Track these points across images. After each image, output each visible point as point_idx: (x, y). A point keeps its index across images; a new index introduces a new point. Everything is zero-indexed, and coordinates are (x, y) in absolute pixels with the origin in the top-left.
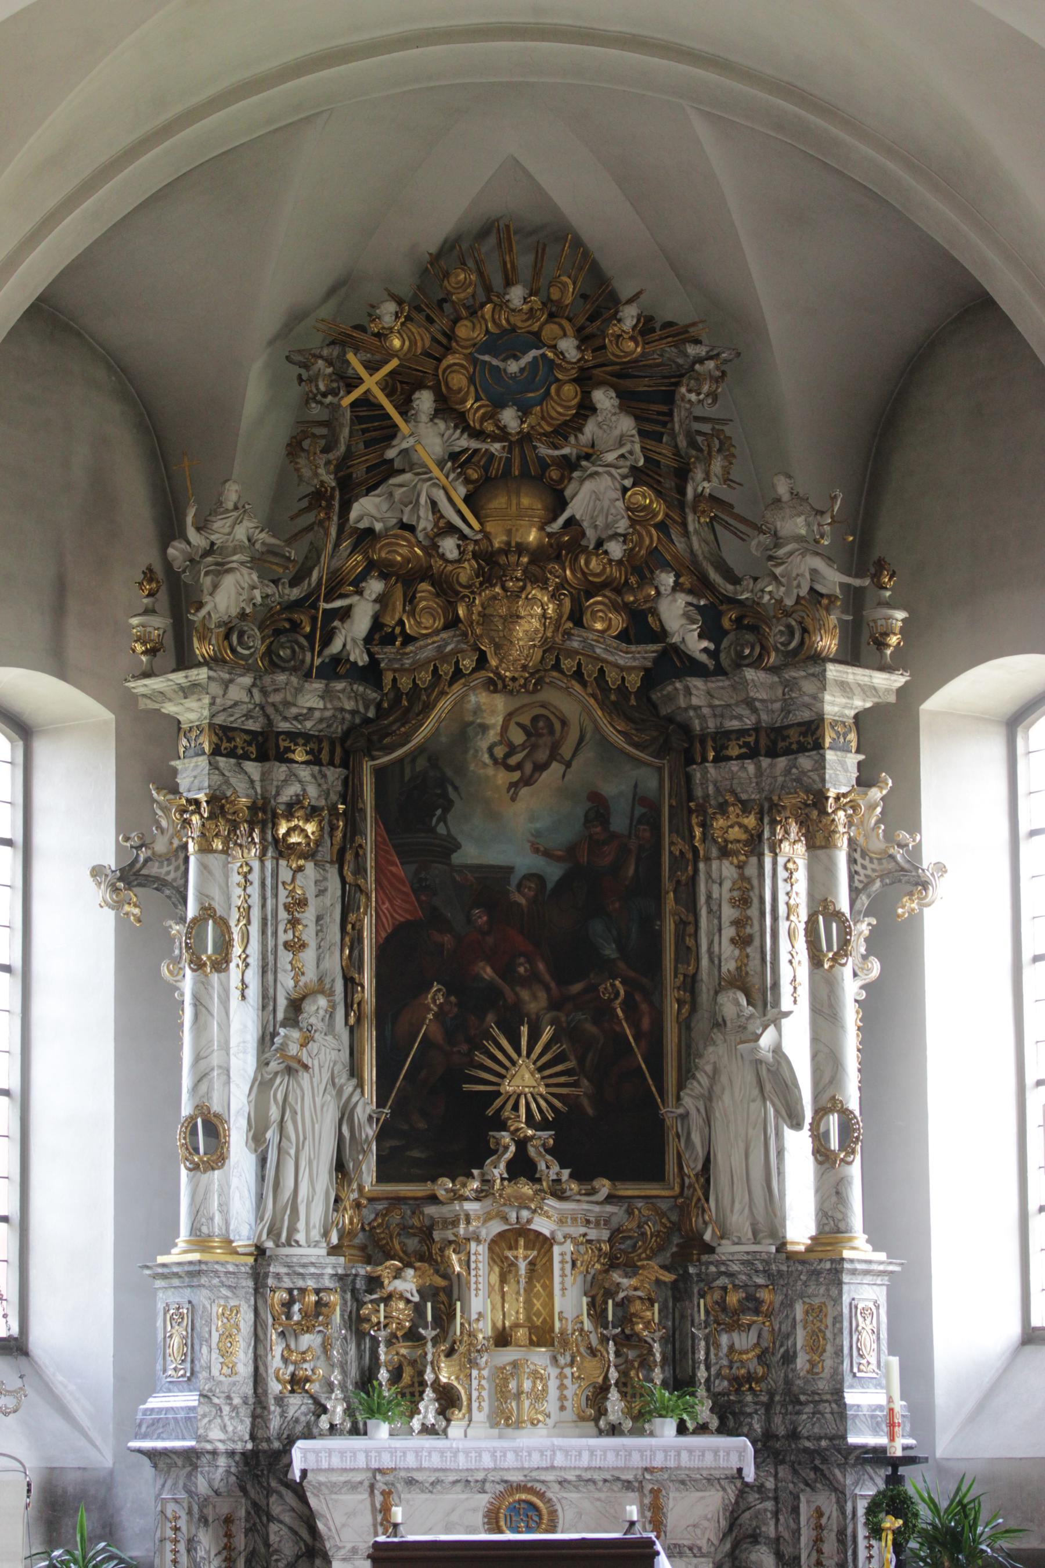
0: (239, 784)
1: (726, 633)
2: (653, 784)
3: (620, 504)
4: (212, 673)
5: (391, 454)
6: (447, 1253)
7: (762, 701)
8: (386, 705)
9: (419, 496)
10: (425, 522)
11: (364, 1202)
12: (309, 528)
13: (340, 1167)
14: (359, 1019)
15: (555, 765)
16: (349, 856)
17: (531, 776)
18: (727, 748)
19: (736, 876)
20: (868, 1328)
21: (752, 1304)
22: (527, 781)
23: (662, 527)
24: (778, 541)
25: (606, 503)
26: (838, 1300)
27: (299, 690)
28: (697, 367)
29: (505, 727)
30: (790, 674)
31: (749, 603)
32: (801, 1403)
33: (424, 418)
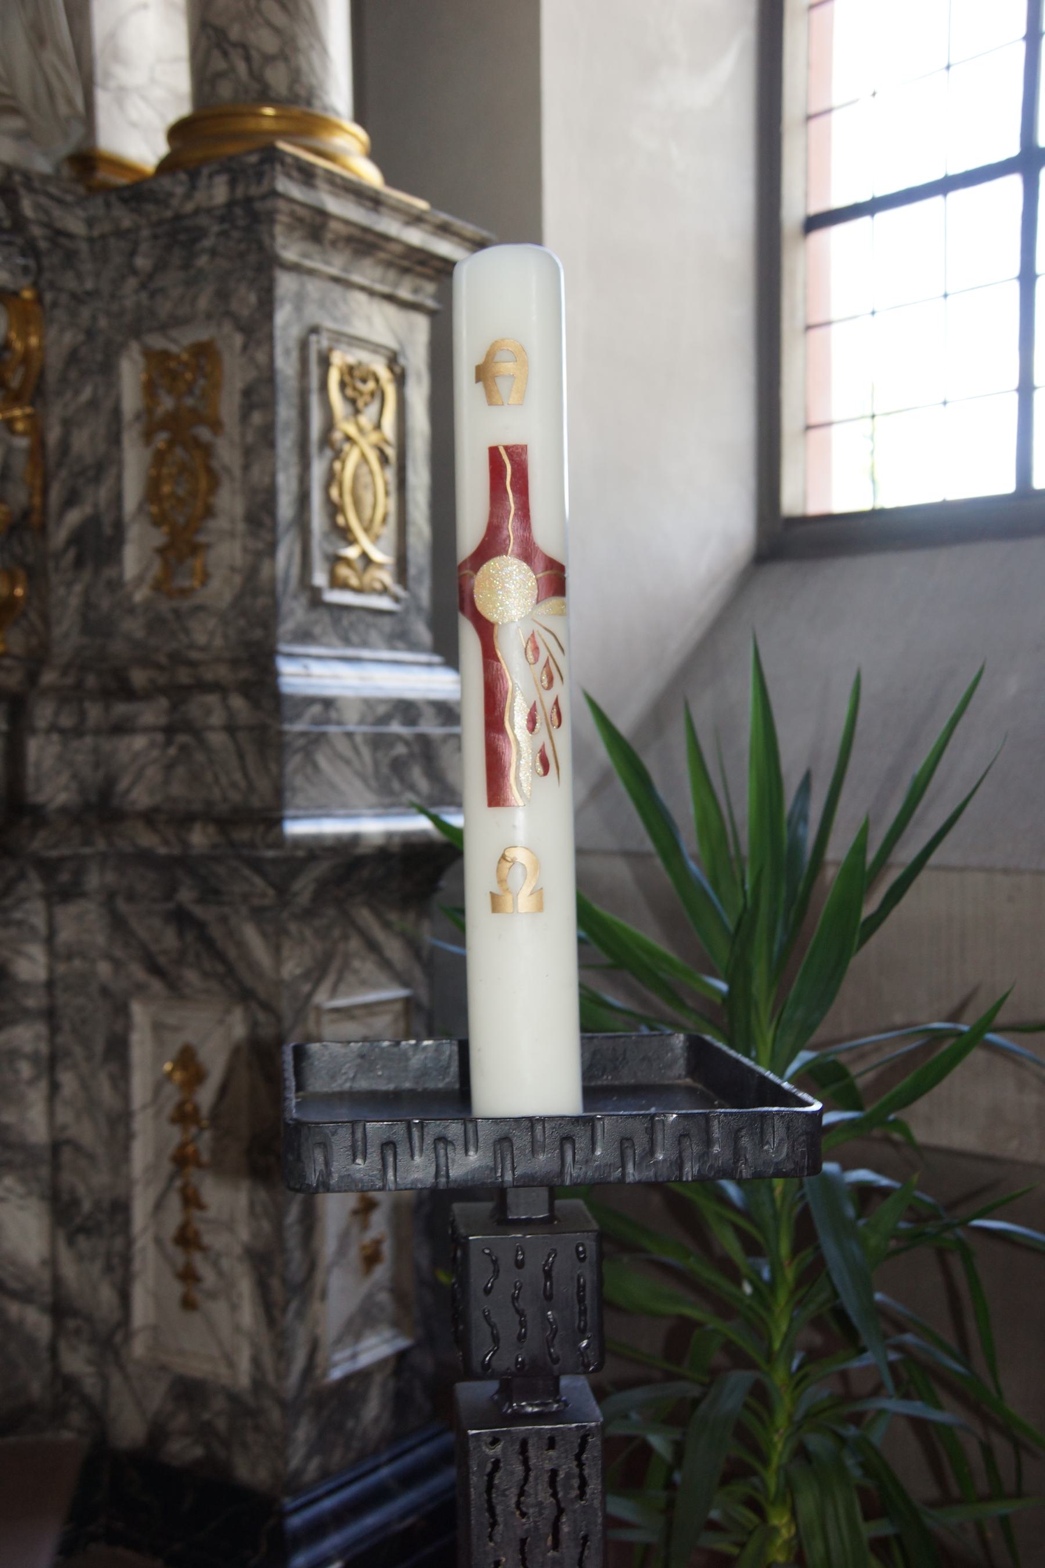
20: (366, 444)
26: (258, 329)
32: (129, 694)
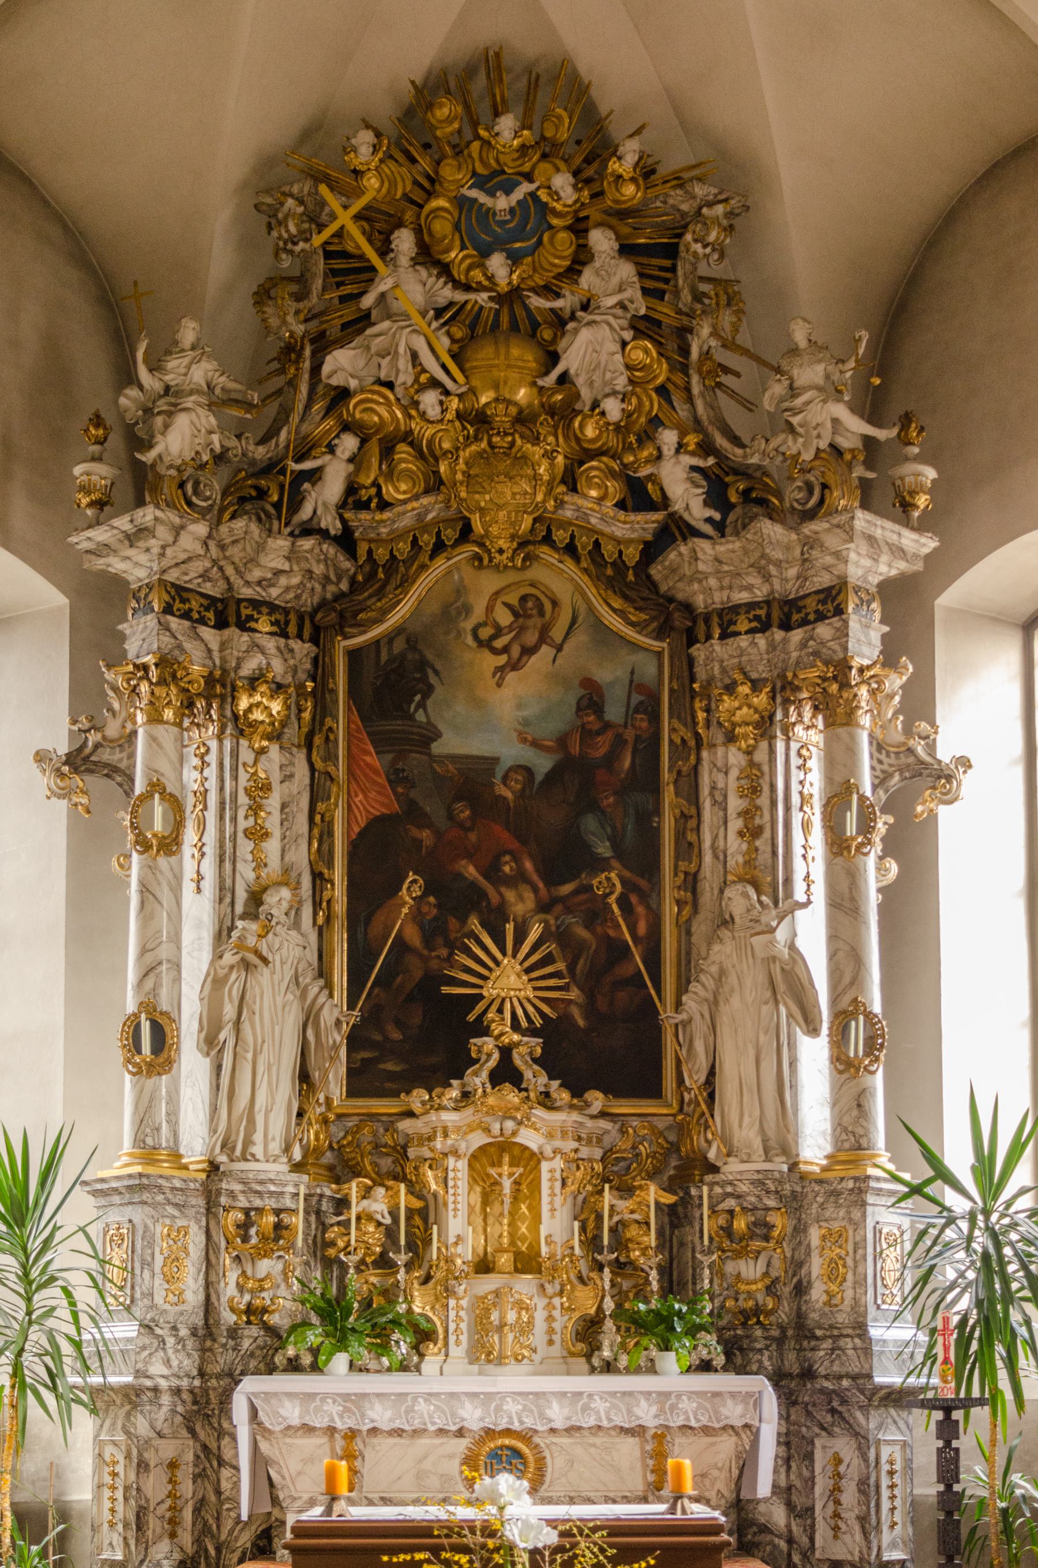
0: (194, 650)
1: (732, 506)
2: (651, 670)
5: (368, 301)
6: (421, 1170)
8: (360, 578)
10: (405, 376)
11: (332, 1117)
13: (304, 1076)
14: (328, 919)
15: (545, 649)
16: (318, 740)
17: (519, 659)
18: (735, 623)
19: (744, 763)
21: (762, 1229)
23: (662, 391)
25: (604, 357)
28: (705, 210)
29: (490, 609)
31: (758, 474)
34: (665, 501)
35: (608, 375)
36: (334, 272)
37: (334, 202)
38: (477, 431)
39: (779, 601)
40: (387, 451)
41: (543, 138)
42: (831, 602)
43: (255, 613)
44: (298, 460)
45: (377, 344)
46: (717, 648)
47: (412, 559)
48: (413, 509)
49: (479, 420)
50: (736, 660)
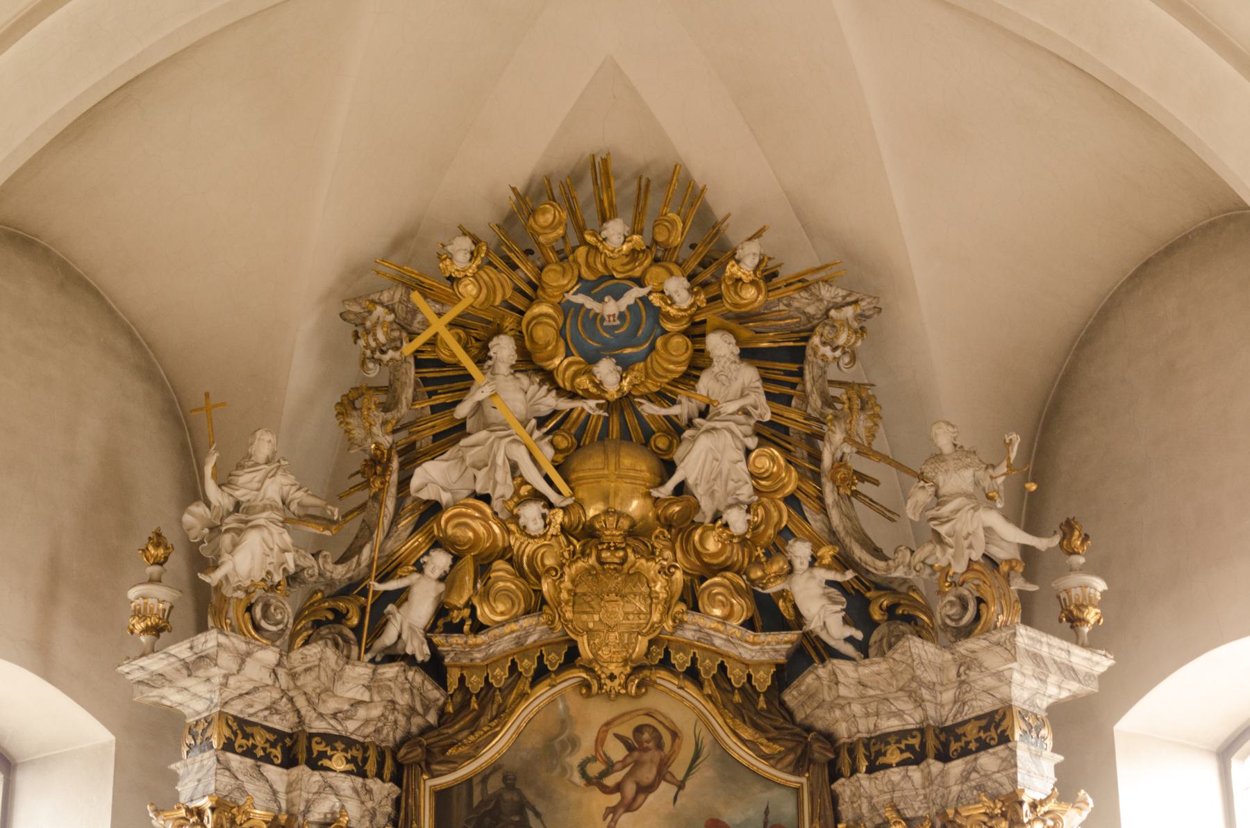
1: (876, 624)
2: (789, 809)
3: (743, 465)
4: (222, 639)
5: (462, 411)
7: (931, 687)
8: (450, 709)
9: (495, 456)
10: (503, 488)
12: (362, 507)
15: (663, 785)
17: (634, 799)
18: (884, 754)
22: (630, 807)
23: (792, 501)
24: (939, 499)
25: (726, 466)
27: (337, 676)
28: (833, 313)
29: (600, 742)
30: (965, 646)
31: (903, 589)
33: (503, 369)
34: (800, 619)
35: (731, 485)
36: (426, 382)
37: (426, 309)
38: (584, 545)
39: (934, 728)
40: (483, 569)
41: (655, 242)
42: (995, 729)
43: (328, 749)
44: (381, 581)
45: (472, 455)
46: (865, 783)
47: (510, 687)
48: (512, 632)
49: (588, 534)
50: (887, 797)
